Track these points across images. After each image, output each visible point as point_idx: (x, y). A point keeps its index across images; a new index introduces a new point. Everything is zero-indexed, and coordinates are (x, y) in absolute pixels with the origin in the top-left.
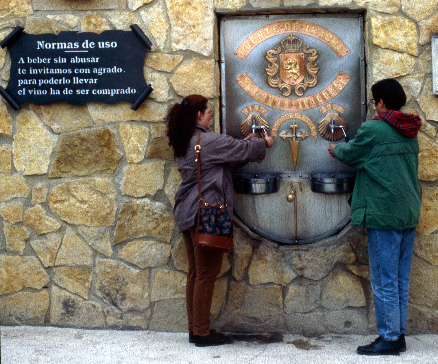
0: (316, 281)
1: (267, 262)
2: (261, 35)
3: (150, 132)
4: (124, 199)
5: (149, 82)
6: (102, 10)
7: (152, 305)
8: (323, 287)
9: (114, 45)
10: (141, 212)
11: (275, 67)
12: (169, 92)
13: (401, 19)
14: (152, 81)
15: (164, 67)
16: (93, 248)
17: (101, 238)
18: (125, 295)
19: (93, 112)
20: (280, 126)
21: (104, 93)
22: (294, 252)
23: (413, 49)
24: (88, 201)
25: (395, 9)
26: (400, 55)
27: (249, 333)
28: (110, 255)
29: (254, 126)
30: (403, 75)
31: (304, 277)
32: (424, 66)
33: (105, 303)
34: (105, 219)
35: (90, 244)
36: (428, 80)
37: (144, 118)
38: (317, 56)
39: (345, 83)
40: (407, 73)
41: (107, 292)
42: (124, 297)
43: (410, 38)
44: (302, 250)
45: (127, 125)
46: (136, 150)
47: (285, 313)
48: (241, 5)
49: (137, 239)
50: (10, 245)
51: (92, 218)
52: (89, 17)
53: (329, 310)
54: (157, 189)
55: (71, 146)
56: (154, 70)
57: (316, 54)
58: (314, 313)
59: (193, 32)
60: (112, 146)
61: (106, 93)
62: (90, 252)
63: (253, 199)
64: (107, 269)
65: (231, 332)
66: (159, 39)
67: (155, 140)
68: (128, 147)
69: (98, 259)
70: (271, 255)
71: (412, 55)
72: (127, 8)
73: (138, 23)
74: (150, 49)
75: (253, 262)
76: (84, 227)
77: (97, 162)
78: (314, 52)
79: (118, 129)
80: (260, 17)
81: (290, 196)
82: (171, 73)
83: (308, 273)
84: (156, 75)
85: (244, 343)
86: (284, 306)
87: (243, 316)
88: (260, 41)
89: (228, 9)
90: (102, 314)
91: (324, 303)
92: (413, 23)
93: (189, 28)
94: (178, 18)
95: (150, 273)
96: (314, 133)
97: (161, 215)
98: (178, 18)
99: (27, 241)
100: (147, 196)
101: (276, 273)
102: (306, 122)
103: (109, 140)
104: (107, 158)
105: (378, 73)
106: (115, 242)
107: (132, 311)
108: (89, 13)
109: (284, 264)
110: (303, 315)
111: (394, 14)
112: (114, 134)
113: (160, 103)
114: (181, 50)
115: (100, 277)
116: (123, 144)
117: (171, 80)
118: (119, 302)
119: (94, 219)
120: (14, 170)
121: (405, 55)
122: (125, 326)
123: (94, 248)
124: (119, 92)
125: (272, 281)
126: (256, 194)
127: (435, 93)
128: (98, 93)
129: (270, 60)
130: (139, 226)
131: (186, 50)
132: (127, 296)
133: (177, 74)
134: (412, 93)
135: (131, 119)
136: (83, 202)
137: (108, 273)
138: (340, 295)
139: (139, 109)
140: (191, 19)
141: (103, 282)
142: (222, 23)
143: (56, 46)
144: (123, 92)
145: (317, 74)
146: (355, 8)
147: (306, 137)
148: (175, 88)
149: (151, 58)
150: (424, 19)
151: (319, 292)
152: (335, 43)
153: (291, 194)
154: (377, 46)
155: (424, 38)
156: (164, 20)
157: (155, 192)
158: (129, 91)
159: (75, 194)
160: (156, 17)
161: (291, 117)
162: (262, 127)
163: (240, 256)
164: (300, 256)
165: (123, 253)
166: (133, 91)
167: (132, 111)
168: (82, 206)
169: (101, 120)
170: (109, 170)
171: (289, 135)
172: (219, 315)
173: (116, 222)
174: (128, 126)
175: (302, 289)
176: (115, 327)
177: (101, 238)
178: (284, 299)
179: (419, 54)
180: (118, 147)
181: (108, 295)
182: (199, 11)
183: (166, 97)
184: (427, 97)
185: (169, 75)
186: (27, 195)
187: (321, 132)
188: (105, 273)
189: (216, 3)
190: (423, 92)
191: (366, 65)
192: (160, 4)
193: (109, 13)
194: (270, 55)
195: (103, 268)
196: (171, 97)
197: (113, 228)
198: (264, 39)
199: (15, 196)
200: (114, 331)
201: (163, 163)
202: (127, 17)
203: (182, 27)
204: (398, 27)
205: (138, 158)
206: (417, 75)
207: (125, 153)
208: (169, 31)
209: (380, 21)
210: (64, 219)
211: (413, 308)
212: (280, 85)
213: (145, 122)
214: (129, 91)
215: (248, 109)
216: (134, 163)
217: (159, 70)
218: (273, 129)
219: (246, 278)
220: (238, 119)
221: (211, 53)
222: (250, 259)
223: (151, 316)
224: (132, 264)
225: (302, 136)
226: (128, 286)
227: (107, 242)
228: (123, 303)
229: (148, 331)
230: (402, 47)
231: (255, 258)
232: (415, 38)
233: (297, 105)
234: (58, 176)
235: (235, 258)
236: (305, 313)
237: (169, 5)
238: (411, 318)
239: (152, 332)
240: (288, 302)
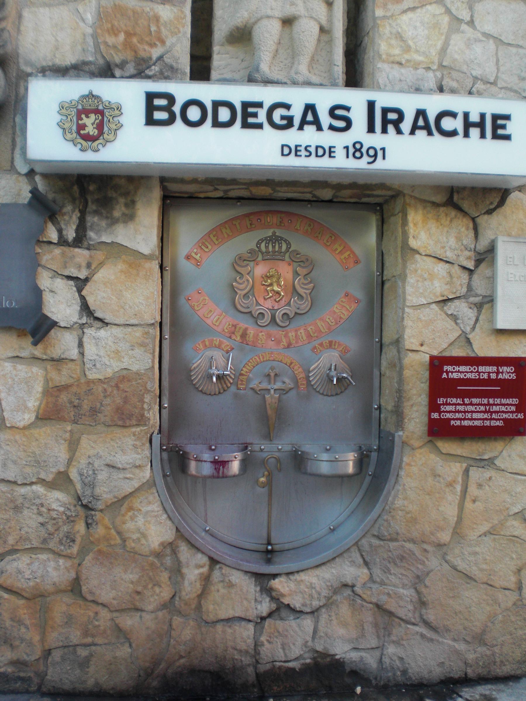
56: (56, 274)
67: (55, 389)
135: (15, 355)
238: (443, 660)
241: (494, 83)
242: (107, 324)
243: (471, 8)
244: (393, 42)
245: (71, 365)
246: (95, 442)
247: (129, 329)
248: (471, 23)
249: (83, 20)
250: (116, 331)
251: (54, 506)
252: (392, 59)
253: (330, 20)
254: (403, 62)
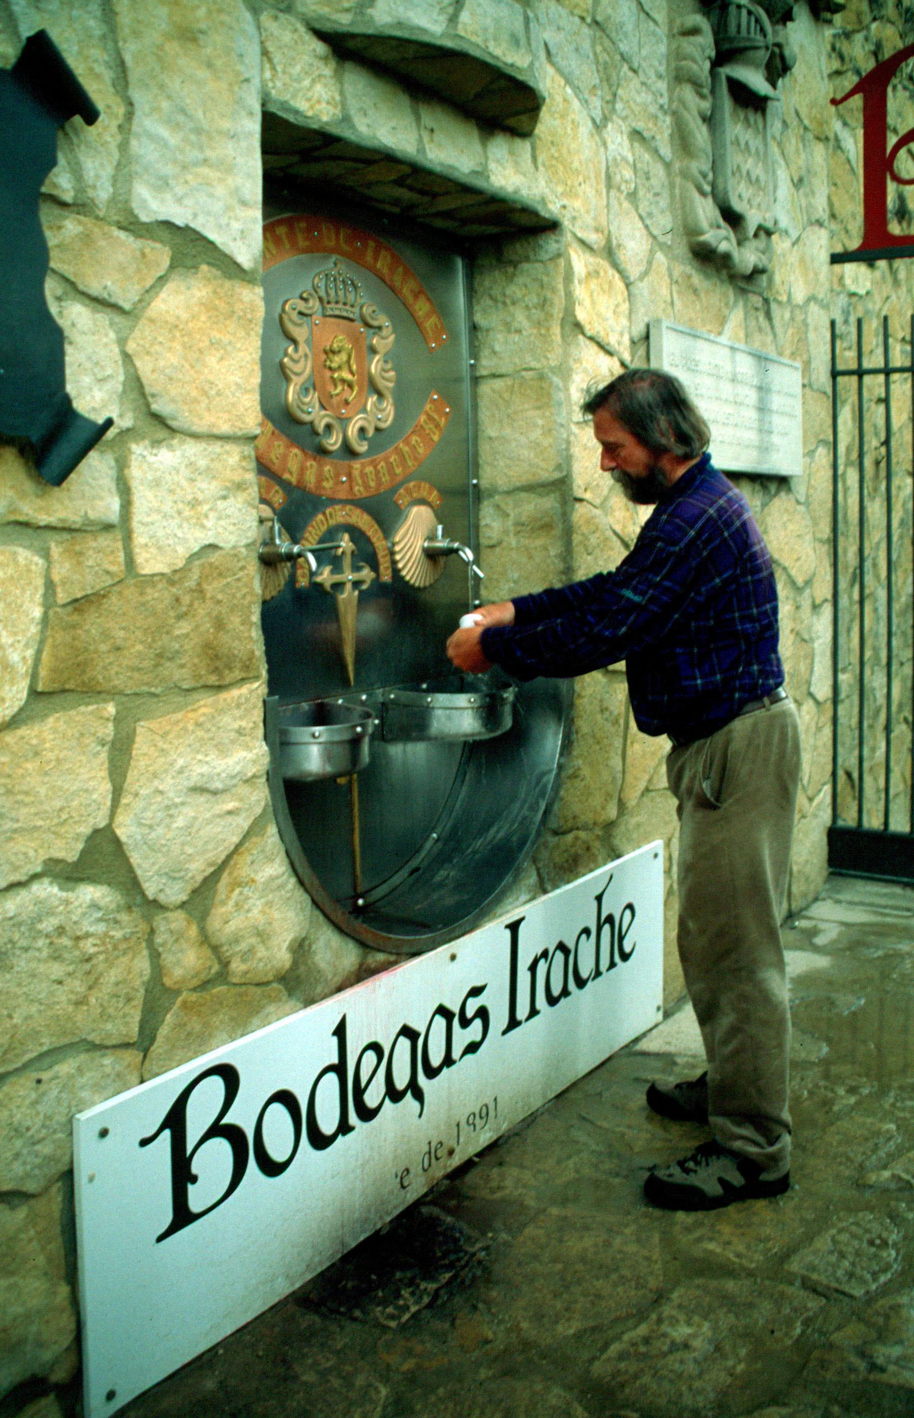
54: (85, 830)
67: (69, 608)
89: (297, 112)
133: (152, 321)
157: (80, 846)
201: (111, 709)
242: (173, 431)
245: (104, 541)
246: (164, 735)
247: (217, 447)
250: (192, 449)
251: (87, 926)
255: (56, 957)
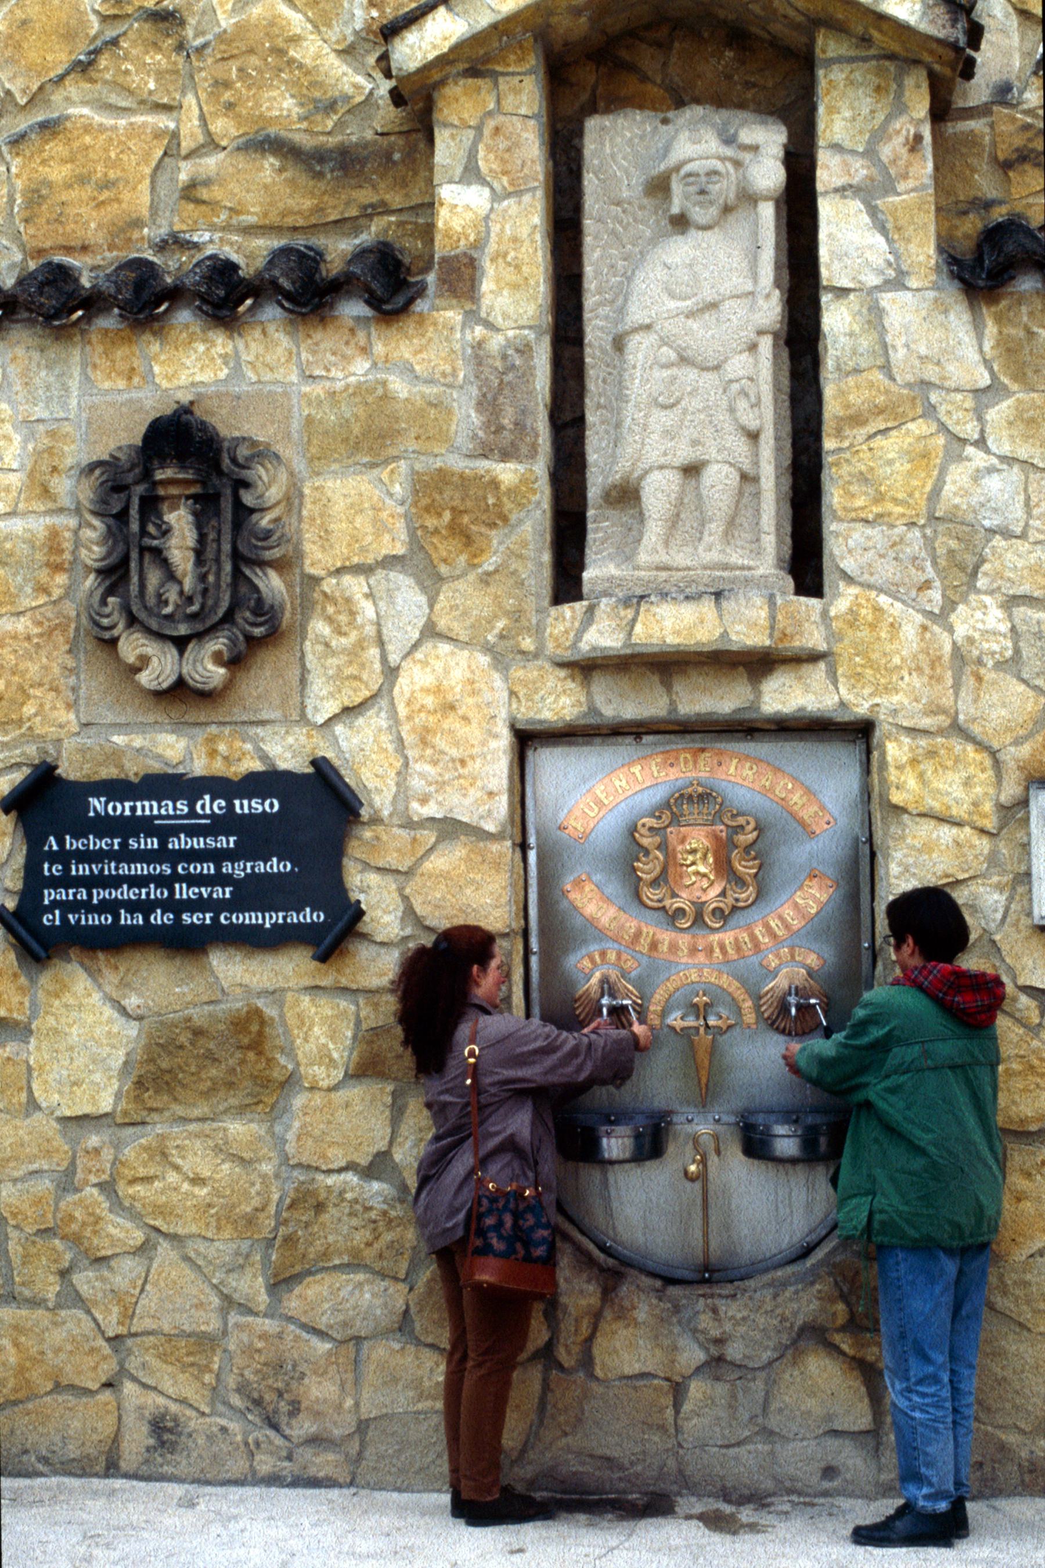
0: (754, 1369)
1: (636, 1324)
2: (624, 783)
3: (358, 1015)
4: (295, 1173)
5: (354, 896)
6: (244, 723)
7: (363, 1427)
8: (771, 1383)
9: (272, 806)
10: (335, 1205)
11: (657, 858)
12: (402, 919)
13: (958, 745)
14: (362, 891)
15: (391, 860)
16: (221, 1292)
17: (242, 1267)
18: (299, 1402)
19: (223, 967)
20: (667, 1000)
21: (247, 922)
22: (702, 1300)
23: (986, 816)
24: (210, 1178)
25: (943, 720)
26: (955, 830)
27: (594, 1494)
28: (262, 1308)
29: (605, 1001)
30: (961, 877)
31: (725, 1361)
32: (1011, 858)
33: (250, 1422)
34: (250, 1221)
35: (214, 1281)
36: (1020, 890)
37: (344, 982)
38: (755, 834)
39: (824, 897)
40: (971, 873)
41: (256, 1395)
42: (295, 1409)
43: (978, 790)
44: (720, 1296)
45: (302, 997)
46: (325, 1058)
47: (680, 1446)
48: (576, 711)
49: (326, 1269)
50: (23, 1284)
51: (218, 1220)
52: (211, 740)
53: (786, 1439)
54: (374, 1150)
55: (170, 1047)
56: (367, 866)
57: (755, 829)
58: (750, 1447)
59: (460, 777)
60: (267, 1046)
61: (254, 921)
62: (216, 1301)
63: (605, 1174)
64: (256, 1340)
65: (551, 1490)
66: (379, 791)
68: (305, 1049)
69: (234, 1318)
70: (647, 1308)
71: (983, 831)
72: (303, 718)
73: (330, 755)
74: (358, 815)
75: (603, 1326)
76: (199, 1240)
77: (230, 1085)
78: (748, 823)
79: (281, 1007)
80: (620, 739)
81: (693, 1168)
82: (409, 873)
83: (734, 1351)
84: (373, 878)
85: (582, 1517)
86: (677, 1430)
87: (579, 1454)
88: (622, 798)
89: (545, 721)
90: (242, 1447)
91: (774, 1422)
92: (985, 755)
93: (450, 765)
94: (424, 742)
95: (358, 1351)
96: (750, 1018)
97: (385, 1213)
98: (424, 742)
99: (64, 1274)
100: (350, 1167)
101: (658, 1352)
102: (730, 990)
103: (260, 1033)
104: (256, 1077)
105: (902, 873)
106: (275, 1276)
107: (314, 1441)
108: (213, 729)
109: (677, 1330)
110: (724, 1451)
111: (941, 732)
112: (272, 1019)
113: (382, 944)
114: (432, 819)
115: (239, 1361)
116: (293, 1042)
117: (408, 891)
118: (283, 1420)
119: (223, 1222)
120: (33, 1105)
121: (967, 830)
122: (298, 1477)
123: (225, 1291)
124: (285, 918)
125: (649, 1368)
126: (612, 1163)
127: (1037, 921)
128: (234, 920)
129: (645, 842)
130: (331, 1239)
131: (445, 819)
132: (303, 1406)
133: (422, 875)
134: (983, 922)
135: (313, 984)
136: (197, 1181)
137: (259, 1351)
138: (811, 1403)
139: (332, 959)
140: (457, 744)
141: (246, 1373)
142: (530, 753)
143: (133, 809)
144: (294, 918)
145: (756, 875)
146: (847, 718)
147: (730, 1027)
148: (419, 910)
149: (359, 839)
150: (1010, 745)
151: (760, 1396)
152: (800, 802)
153: (694, 1161)
154: (899, 810)
155: (1011, 790)
156: (391, 747)
157: (370, 1158)
158: (309, 916)
159: (179, 1161)
160: (371, 739)
161: (694, 977)
162: (625, 1002)
163: (571, 1309)
164: (715, 1311)
165: (293, 1303)
166: (318, 917)
167: (315, 963)
168: (197, 1190)
169: (241, 985)
170: (261, 1106)
171: (691, 1022)
172: (523, 1451)
173: (276, 1229)
174: (306, 1000)
175: (721, 1389)
176: (274, 1480)
177: (242, 1267)
178: (677, 1412)
179: (1001, 829)
180: (282, 1050)
181: (258, 1402)
182: (474, 725)
183: (396, 931)
184: (1019, 932)
185: (402, 878)
186: (65, 1164)
187: (766, 1015)
188: (250, 1351)
189: (514, 706)
190: (1008, 919)
191: (873, 855)
192: (381, 709)
193: (259, 730)
194: (644, 831)
195: (245, 1339)
196: (408, 931)
197: (270, 1243)
198: (630, 793)
199: (35, 1166)
200: (273, 1489)
201: (390, 1088)
202: (303, 739)
203: (435, 763)
204: (950, 763)
205: (329, 1076)
206: (995, 879)
207: (298, 1064)
208: (403, 774)
209: (906, 748)
210: (152, 1222)
211: (986, 1433)
212: (667, 903)
213: (345, 990)
214: (309, 916)
215: (592, 960)
216: (319, 1089)
217: (380, 865)
218: (652, 1008)
219: (587, 1362)
220: (569, 984)
221: (503, 826)
222: (597, 1317)
223: (360, 1453)
224: (314, 1329)
225: (720, 1023)
226: (306, 1381)
227: (255, 1276)
228: (294, 1422)
229: (353, 1490)
230: (958, 812)
231: (608, 1314)
232: (991, 791)
233: (709, 950)
234: (139, 1120)
235: (561, 1316)
236: (727, 1447)
237: (402, 711)
238: (980, 1459)
239: (363, 1492)
240: (687, 1419)
241: (1023, 536)
243: (980, 419)
244: (854, 488)
248: (981, 443)
249: (391, 495)
252: (853, 515)
253: (756, 463)
254: (871, 517)
255: (352, 1214)
